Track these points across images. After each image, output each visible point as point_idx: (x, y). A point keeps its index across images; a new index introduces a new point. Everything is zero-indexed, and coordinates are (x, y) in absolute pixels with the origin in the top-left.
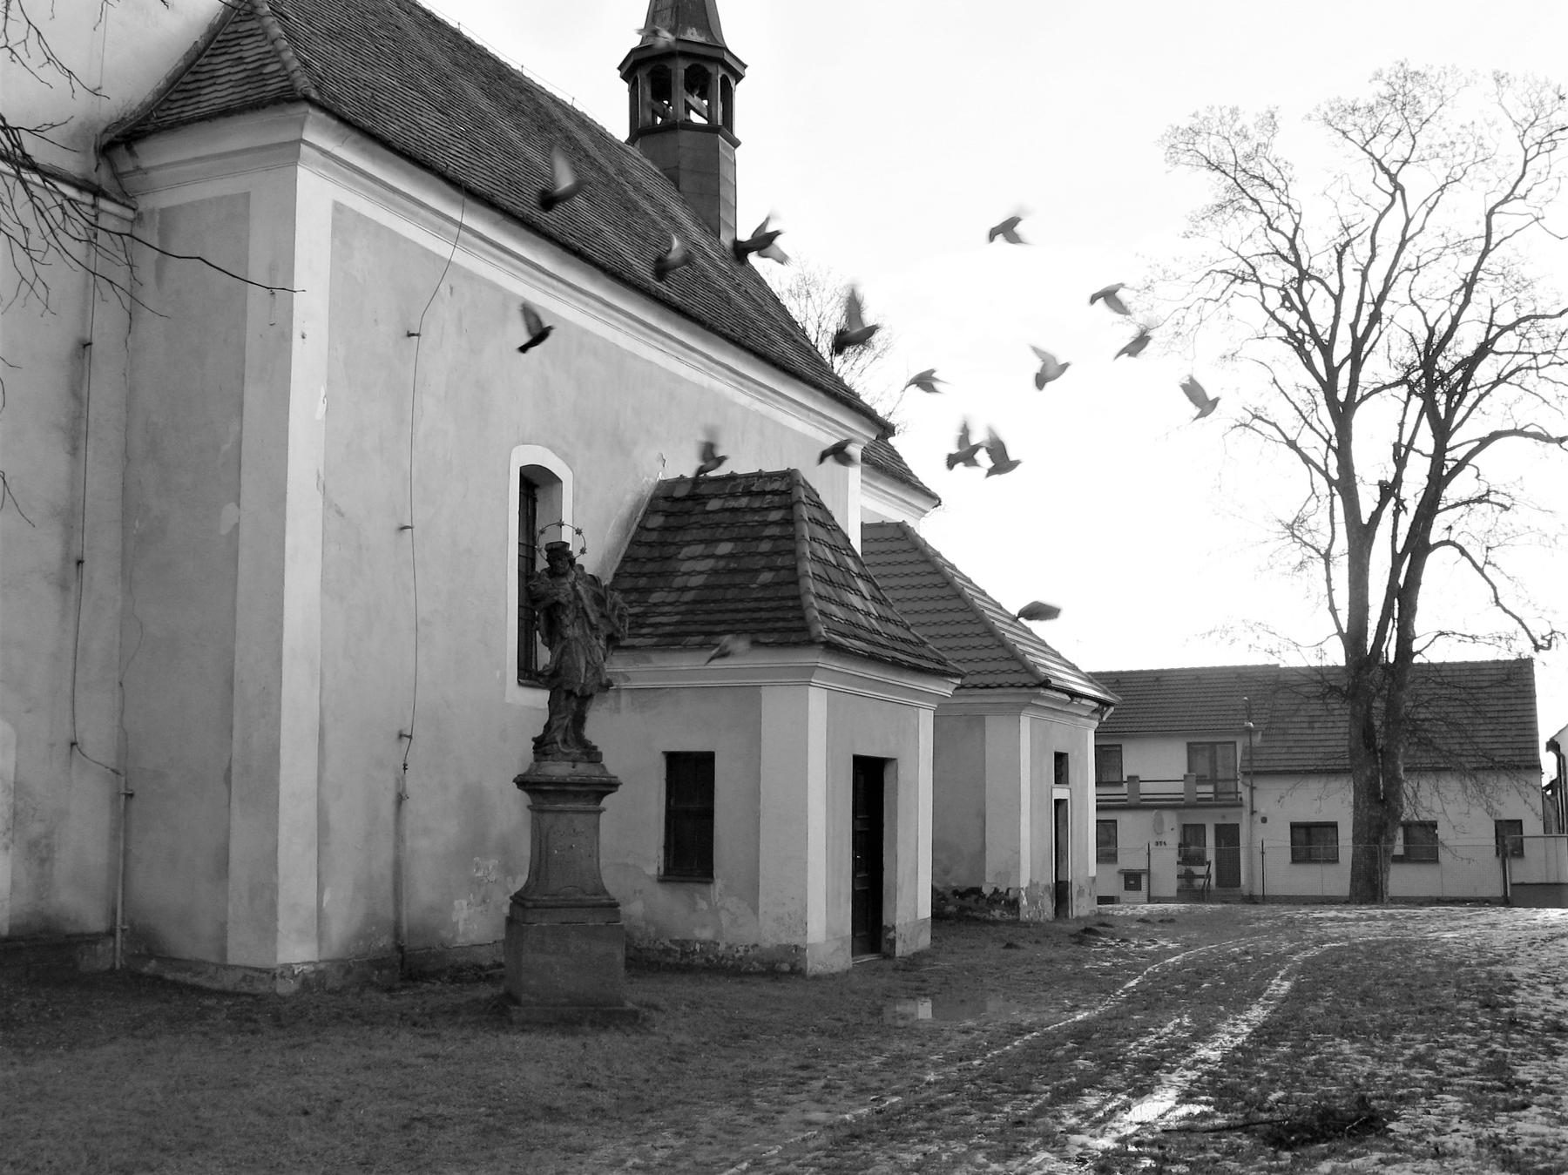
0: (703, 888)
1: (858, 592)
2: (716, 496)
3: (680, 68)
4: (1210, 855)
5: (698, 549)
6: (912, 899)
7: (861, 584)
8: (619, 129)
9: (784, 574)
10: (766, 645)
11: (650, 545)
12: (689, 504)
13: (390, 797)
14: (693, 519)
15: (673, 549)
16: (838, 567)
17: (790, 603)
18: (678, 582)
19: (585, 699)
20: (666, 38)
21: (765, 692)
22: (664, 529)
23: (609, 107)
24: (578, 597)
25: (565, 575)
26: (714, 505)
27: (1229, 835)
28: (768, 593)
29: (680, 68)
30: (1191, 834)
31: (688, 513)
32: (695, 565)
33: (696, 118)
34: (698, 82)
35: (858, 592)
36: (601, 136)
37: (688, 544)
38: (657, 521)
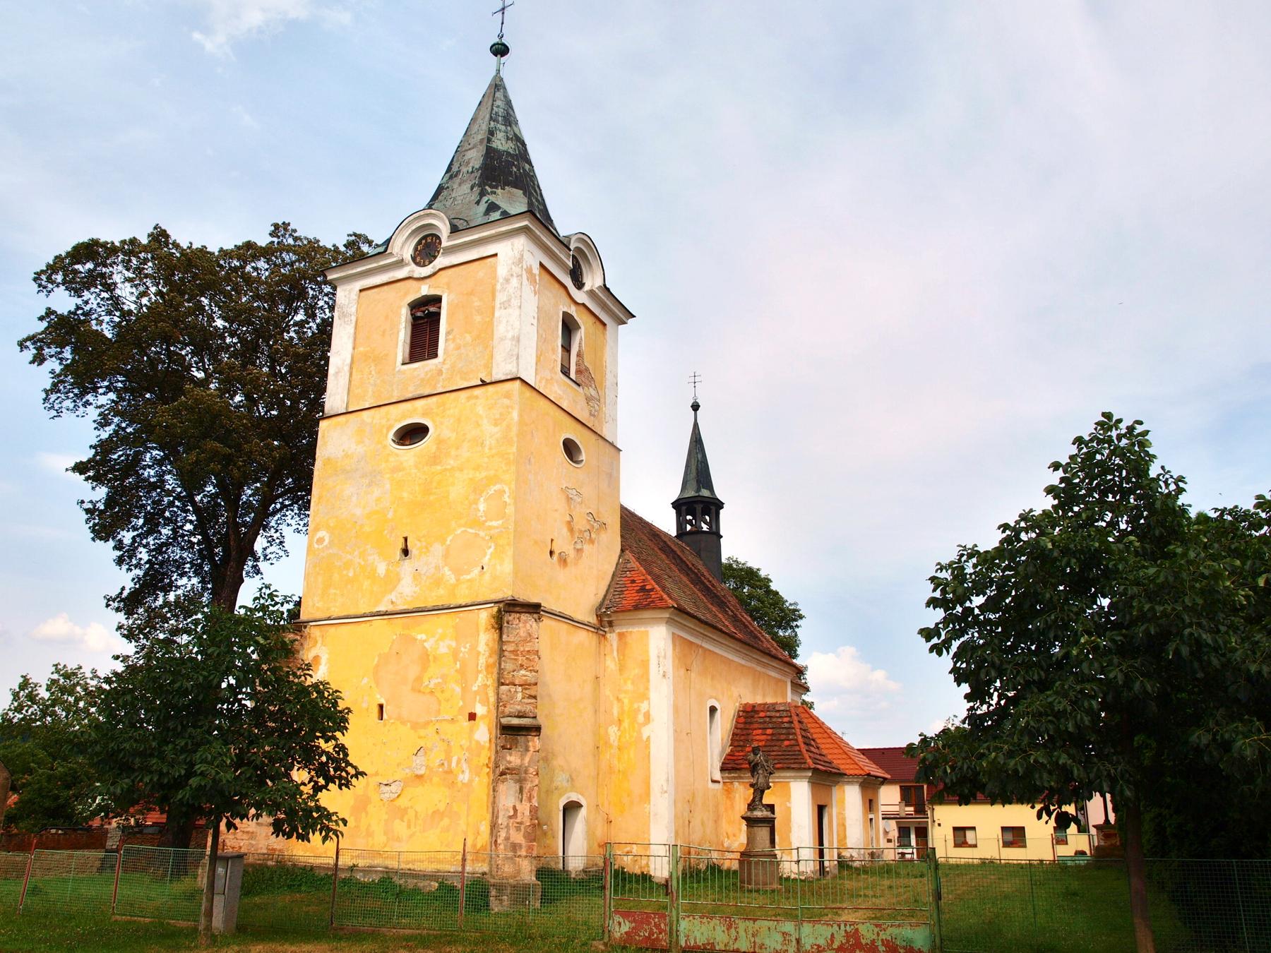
3: (699, 508)
4: (913, 843)
6: (831, 857)
19: (763, 792)
20: (692, 494)
23: (667, 522)
26: (762, 714)
27: (922, 833)
29: (699, 508)
30: (904, 832)
32: (759, 738)
34: (706, 511)
36: (666, 535)
38: (742, 720)
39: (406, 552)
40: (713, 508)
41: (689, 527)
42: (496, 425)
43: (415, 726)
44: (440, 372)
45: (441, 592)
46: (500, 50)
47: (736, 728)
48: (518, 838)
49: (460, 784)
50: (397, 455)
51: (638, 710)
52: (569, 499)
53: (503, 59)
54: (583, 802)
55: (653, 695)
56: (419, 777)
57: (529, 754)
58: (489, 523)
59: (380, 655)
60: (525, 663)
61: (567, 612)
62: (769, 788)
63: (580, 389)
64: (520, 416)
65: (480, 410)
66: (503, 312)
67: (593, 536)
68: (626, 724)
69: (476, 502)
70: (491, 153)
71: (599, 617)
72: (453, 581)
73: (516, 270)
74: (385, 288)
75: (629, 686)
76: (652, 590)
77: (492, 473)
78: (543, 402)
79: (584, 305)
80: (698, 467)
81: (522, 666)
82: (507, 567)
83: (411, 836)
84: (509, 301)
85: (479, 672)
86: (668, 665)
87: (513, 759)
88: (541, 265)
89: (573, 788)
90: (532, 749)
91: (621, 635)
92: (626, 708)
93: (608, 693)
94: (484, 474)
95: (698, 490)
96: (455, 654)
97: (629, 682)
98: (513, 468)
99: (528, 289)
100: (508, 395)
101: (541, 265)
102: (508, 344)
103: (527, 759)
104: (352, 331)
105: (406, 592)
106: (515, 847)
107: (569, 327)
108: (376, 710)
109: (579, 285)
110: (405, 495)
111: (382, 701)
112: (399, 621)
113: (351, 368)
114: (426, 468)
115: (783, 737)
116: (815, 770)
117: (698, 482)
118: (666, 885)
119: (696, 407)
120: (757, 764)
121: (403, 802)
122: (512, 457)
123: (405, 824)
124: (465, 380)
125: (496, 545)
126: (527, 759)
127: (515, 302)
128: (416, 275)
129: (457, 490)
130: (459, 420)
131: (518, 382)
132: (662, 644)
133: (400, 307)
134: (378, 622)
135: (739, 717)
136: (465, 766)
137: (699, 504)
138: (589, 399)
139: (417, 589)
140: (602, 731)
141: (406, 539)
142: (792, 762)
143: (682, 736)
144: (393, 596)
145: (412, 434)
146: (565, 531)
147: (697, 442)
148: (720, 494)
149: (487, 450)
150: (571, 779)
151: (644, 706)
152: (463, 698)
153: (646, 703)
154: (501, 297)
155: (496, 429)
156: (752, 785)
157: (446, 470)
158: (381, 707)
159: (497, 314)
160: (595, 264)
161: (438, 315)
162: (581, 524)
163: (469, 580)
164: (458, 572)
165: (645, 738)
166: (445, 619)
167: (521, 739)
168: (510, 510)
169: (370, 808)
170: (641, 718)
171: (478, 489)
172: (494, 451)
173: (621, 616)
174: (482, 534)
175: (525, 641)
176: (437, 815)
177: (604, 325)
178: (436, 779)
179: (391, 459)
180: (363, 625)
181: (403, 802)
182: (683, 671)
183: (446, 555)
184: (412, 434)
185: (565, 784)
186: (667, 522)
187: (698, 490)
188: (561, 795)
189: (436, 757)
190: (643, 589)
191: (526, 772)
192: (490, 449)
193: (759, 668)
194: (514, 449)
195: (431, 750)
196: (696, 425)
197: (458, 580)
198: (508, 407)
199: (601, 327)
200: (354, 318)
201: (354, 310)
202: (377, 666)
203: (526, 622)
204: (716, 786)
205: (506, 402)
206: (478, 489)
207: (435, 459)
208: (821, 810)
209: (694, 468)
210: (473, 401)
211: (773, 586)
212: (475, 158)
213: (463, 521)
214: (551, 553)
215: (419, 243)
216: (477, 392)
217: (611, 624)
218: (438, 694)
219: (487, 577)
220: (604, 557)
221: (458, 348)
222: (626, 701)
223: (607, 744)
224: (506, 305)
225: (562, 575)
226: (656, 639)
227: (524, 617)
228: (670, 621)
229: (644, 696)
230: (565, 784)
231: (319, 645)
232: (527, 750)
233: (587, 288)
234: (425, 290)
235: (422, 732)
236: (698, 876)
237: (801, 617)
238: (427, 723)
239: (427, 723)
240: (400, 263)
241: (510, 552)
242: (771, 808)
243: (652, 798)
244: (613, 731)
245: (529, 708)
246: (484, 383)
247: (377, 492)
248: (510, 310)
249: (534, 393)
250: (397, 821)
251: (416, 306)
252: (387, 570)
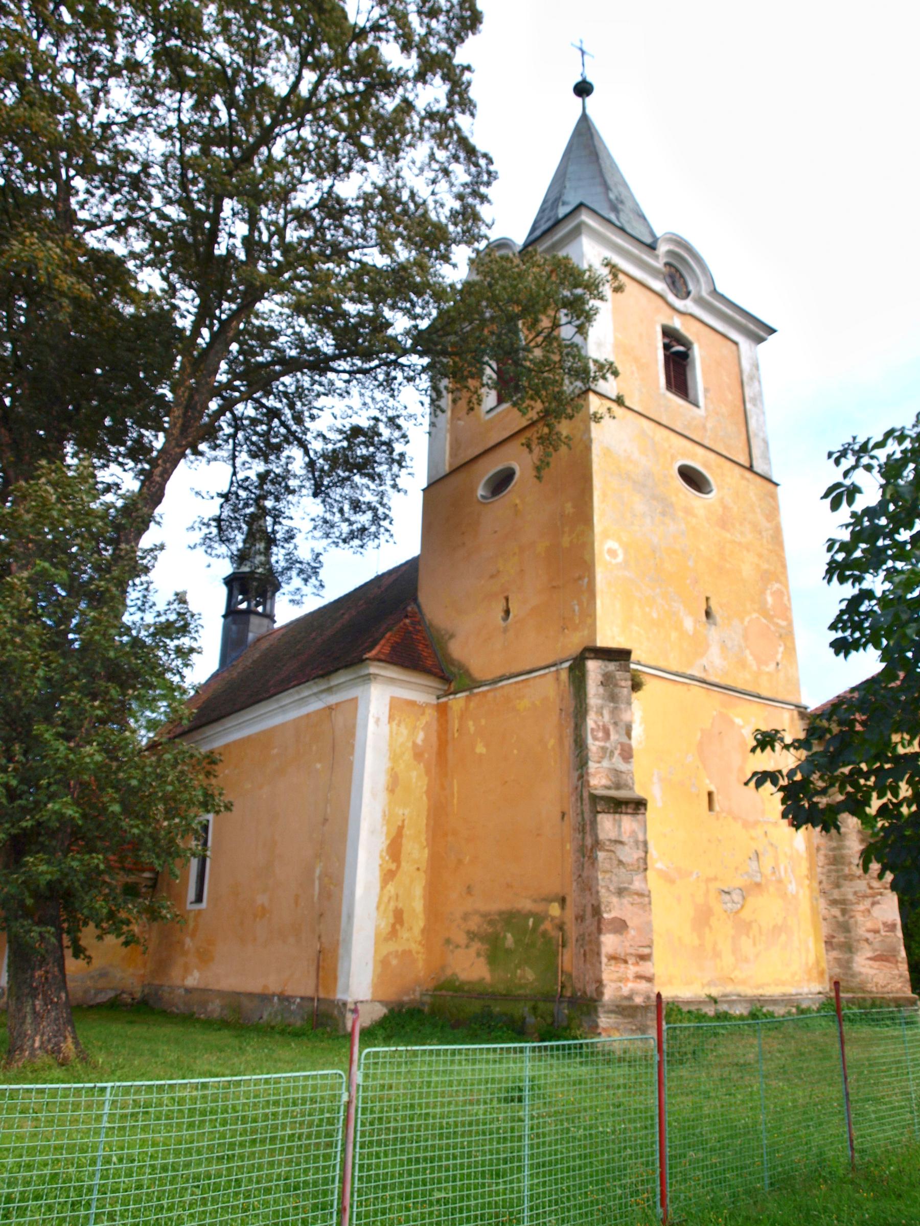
43: (746, 825)
46: (583, 89)
53: (588, 100)
56: (758, 885)
58: (776, 620)
59: (702, 730)
111: (712, 788)
112: (717, 696)
141: (707, 599)
144: (704, 661)
145: (693, 478)
158: (710, 794)
169: (713, 921)
176: (777, 930)
178: (772, 889)
180: (680, 686)
181: (745, 914)
184: (693, 478)
250: (744, 938)
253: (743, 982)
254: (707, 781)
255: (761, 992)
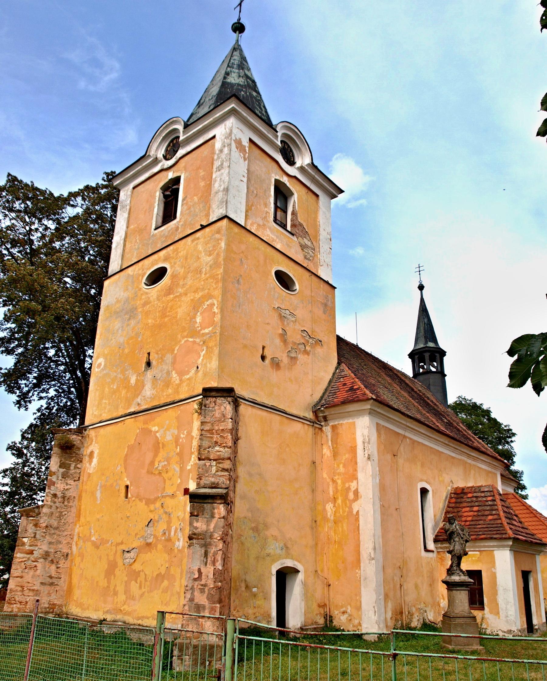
0: (482, 611)
1: (515, 520)
2: (470, 493)
3: (427, 355)
5: (468, 509)
7: (515, 518)
8: (410, 374)
9: (496, 517)
10: (495, 538)
11: (452, 507)
12: (462, 495)
13: (399, 586)
14: (464, 500)
15: (460, 509)
16: (509, 513)
17: (499, 525)
18: (464, 519)
21: (495, 552)
22: (456, 503)
23: (406, 367)
24: (457, 530)
25: (453, 524)
26: (470, 495)
28: (492, 522)
29: (427, 355)
31: (462, 498)
32: (467, 514)
33: (434, 369)
35: (515, 520)
37: (464, 507)
38: (453, 500)
39: (149, 364)
40: (437, 355)
41: (421, 370)
42: (210, 255)
43: (149, 502)
44: (177, 228)
45: (170, 391)
46: (239, 28)
47: (448, 507)
48: (202, 599)
49: (176, 551)
50: (147, 293)
51: (349, 488)
52: (282, 318)
54: (299, 567)
55: (360, 475)
56: (149, 545)
57: (214, 521)
58: (203, 332)
60: (220, 440)
61: (281, 407)
62: (466, 554)
63: (295, 238)
64: (228, 245)
65: (200, 248)
66: (218, 173)
67: (308, 348)
68: (339, 501)
69: (195, 317)
70: (224, 84)
71: (315, 413)
72: (178, 382)
73: (227, 141)
74: (148, 182)
75: (342, 469)
76: (358, 389)
77: (206, 291)
78: (252, 239)
79: (295, 177)
80: (425, 327)
81: (216, 443)
82: (214, 364)
83: (142, 595)
84: (222, 164)
85: (192, 453)
86: (373, 449)
87: (200, 525)
88: (251, 140)
89: (288, 556)
90: (217, 516)
91: (334, 428)
92: (339, 488)
93: (325, 475)
94: (201, 294)
95: (426, 343)
96: (177, 440)
97: (341, 466)
98: (220, 285)
99: (236, 154)
100: (218, 232)
101: (251, 140)
102: (221, 194)
103: (212, 526)
104: (127, 216)
105: (149, 395)
106: (199, 608)
107: (282, 194)
108: (123, 490)
109: (291, 163)
110: (150, 321)
111: (128, 483)
112: (142, 418)
113: (125, 240)
114: (164, 299)
115: (487, 513)
116: (515, 540)
117: (426, 338)
118: (382, 640)
119: (421, 287)
120: (452, 533)
121: (137, 567)
122: (220, 276)
123: (138, 585)
124: (190, 229)
125: (207, 348)
126: (212, 526)
127: (226, 164)
128: (165, 167)
129: (182, 310)
130: (186, 259)
131: (225, 221)
132: (366, 432)
133: (155, 192)
134: (129, 421)
135: (451, 498)
136: (180, 534)
137: (428, 353)
138: (303, 247)
139: (154, 392)
140: (320, 508)
141: (149, 354)
142: (495, 534)
143: (388, 510)
145: (157, 276)
146: (278, 341)
147: (423, 311)
148: (442, 345)
149: (203, 275)
150: (286, 547)
151: (353, 485)
152: (180, 477)
153: (355, 482)
154: (217, 164)
155: (209, 259)
156: (449, 552)
157: (176, 297)
158: (127, 487)
159: (214, 176)
160: (304, 149)
161: (178, 190)
162: (295, 337)
163: (188, 379)
164: (181, 374)
165: (355, 512)
166: (171, 413)
167: (207, 506)
168: (217, 318)
169: (117, 572)
170: (351, 496)
171: (196, 306)
172: (208, 275)
173: (333, 411)
174: (198, 340)
175: (220, 421)
176: (160, 577)
177: (317, 196)
178: (160, 546)
179: (143, 297)
180: (120, 424)
181: (137, 567)
182: (389, 457)
183: (174, 363)
184: (157, 276)
185: (278, 551)
186: (406, 367)
187: (426, 343)
188: (274, 561)
189: (162, 526)
190: (352, 389)
191: (211, 537)
192: (206, 274)
193: (469, 461)
194: (221, 270)
195: (158, 521)
196: (422, 300)
197: (181, 380)
198: (218, 240)
199: (314, 197)
200: (128, 207)
201: (128, 202)
202: (126, 455)
203: (221, 405)
204: (430, 555)
205: (217, 236)
206: (196, 306)
207: (169, 291)
208: (525, 576)
209: (422, 328)
210: (196, 242)
211: (493, 415)
212: (215, 90)
213: (185, 334)
214: (263, 358)
215: (169, 145)
216: (198, 234)
217: (325, 419)
218: (164, 475)
219: (200, 374)
220: (321, 369)
221: (189, 208)
222: (339, 482)
223: (325, 519)
224: (219, 169)
225: (274, 376)
226: (362, 428)
227: (219, 401)
228: (371, 412)
229: (354, 477)
230: (278, 551)
231: (94, 443)
232: (213, 516)
233: (298, 165)
234: (171, 175)
235: (152, 507)
236: (405, 635)
237: (514, 434)
238: (156, 499)
239: (156, 499)
240: (156, 161)
241: (216, 351)
242: (476, 575)
243: (362, 565)
244: (329, 507)
245: (222, 479)
246: (203, 227)
247: (133, 322)
248: (222, 171)
249: (243, 231)
251: (165, 189)
252: (137, 380)
253: (128, 614)
254: (126, 479)
255: (139, 622)
